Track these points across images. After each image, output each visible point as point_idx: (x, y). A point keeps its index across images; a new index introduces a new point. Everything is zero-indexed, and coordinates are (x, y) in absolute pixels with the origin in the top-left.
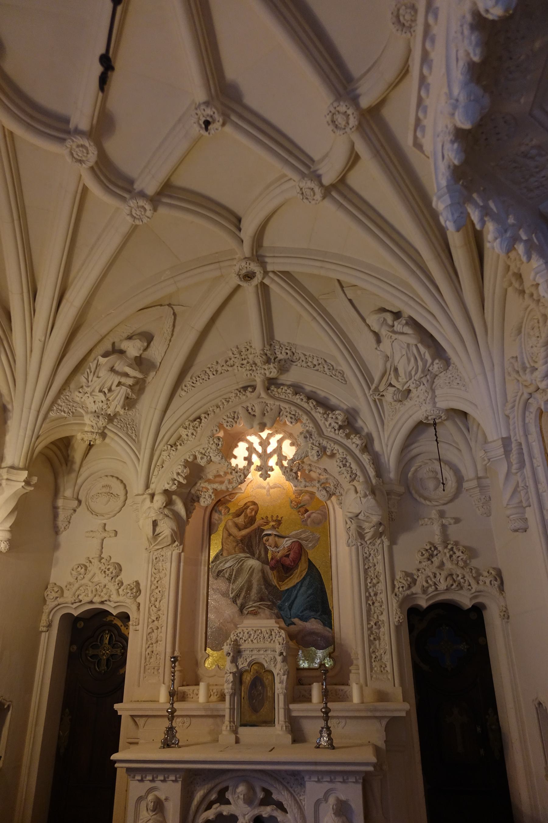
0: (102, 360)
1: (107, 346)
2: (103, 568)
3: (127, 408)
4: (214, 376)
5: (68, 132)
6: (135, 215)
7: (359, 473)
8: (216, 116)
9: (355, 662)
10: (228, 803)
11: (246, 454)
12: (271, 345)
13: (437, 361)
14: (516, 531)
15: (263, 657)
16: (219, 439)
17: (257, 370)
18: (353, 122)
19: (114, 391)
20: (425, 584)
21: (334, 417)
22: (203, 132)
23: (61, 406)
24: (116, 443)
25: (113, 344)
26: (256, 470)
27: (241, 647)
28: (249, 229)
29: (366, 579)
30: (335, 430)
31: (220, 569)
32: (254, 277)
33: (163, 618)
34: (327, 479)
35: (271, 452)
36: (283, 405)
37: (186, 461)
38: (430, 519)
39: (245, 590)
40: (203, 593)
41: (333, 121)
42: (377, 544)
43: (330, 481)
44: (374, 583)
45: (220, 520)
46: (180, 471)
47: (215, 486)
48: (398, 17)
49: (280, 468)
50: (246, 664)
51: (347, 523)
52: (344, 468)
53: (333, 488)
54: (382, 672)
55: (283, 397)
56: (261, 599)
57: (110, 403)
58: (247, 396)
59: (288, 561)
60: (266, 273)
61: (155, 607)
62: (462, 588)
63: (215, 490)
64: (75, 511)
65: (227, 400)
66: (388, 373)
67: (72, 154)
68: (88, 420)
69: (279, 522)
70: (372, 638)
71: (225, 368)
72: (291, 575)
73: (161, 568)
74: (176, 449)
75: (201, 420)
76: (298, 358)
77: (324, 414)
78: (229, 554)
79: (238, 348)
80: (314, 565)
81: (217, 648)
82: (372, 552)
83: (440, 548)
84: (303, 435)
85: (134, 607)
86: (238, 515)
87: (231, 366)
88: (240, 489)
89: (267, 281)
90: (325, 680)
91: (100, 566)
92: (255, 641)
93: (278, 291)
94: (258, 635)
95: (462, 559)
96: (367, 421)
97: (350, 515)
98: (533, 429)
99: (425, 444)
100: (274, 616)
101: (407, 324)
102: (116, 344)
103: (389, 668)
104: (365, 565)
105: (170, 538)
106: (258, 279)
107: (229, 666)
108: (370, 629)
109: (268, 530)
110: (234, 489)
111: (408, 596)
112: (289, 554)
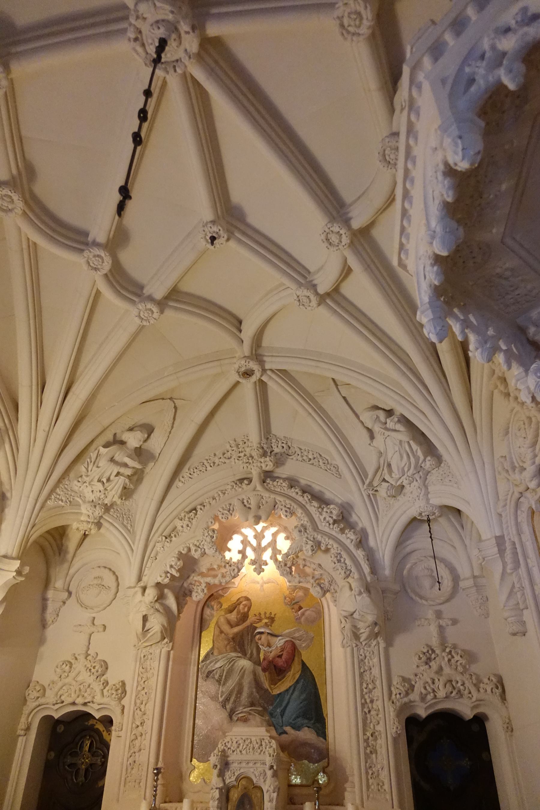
0: (103, 450)
1: (108, 436)
2: (89, 666)
3: (124, 498)
4: (211, 468)
5: (87, 244)
6: (143, 317)
7: (353, 570)
8: (221, 232)
9: (350, 779)
11: (241, 547)
12: (267, 439)
13: (429, 458)
14: (514, 634)
15: (252, 770)
16: (213, 531)
17: (253, 462)
18: (345, 240)
19: (112, 480)
20: (424, 691)
21: (328, 511)
22: (209, 246)
23: (59, 495)
24: (111, 534)
25: (115, 434)
26: (250, 564)
27: (229, 759)
28: (248, 331)
29: (361, 684)
30: (330, 524)
31: (210, 669)
32: (253, 374)
33: (148, 723)
34: (321, 575)
35: (265, 546)
36: (278, 498)
37: (180, 553)
38: (426, 619)
39: (235, 693)
40: (192, 696)
41: (328, 240)
42: (373, 645)
43: (324, 577)
44: (369, 689)
45: (212, 615)
46: (173, 564)
48: (384, 155)
49: (274, 562)
50: (233, 779)
51: (341, 622)
52: (339, 564)
53: (327, 584)
54: (379, 790)
55: (279, 490)
56: (252, 704)
57: (108, 492)
58: (243, 489)
59: (280, 662)
60: (264, 371)
61: (140, 710)
62: (461, 696)
63: (208, 584)
64: (64, 603)
65: (224, 492)
66: (381, 469)
67: (88, 263)
68: (85, 509)
70: (368, 751)
71: (223, 460)
72: (283, 678)
73: (149, 668)
74: (171, 541)
75: (197, 511)
76: (294, 452)
77: (318, 508)
78: (220, 653)
79: (235, 441)
80: (308, 668)
81: (203, 759)
82: (367, 654)
83: (438, 652)
84: (297, 529)
85: (118, 710)
87: (229, 458)
88: (234, 583)
89: (264, 378)
90: (318, 799)
91: (86, 663)
92: (244, 752)
93: (275, 387)
94: (247, 745)
95: (461, 664)
96: (361, 516)
97: (345, 614)
98: (526, 529)
99: (420, 540)
100: (265, 724)
101: (399, 421)
102: (117, 435)
103: (386, 787)
104: (360, 668)
105: (159, 635)
106: (257, 377)
107: (215, 781)
108: (366, 741)
109: (261, 627)
110: (227, 583)
111: (405, 704)
112: (282, 655)
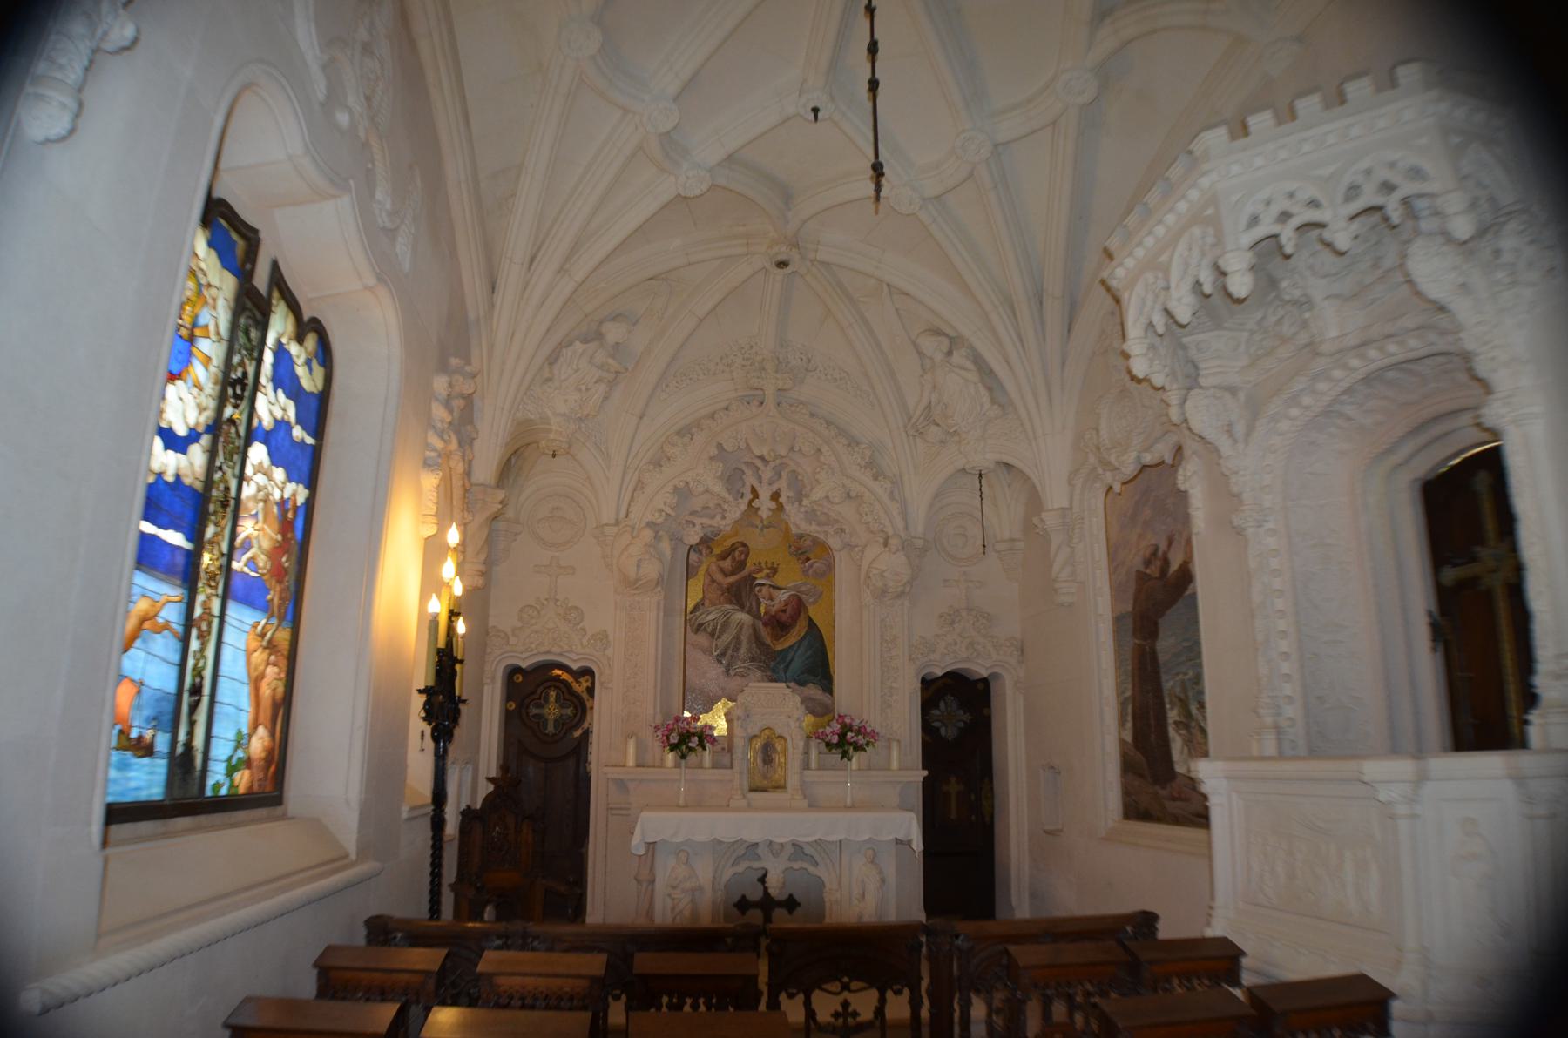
10: (759, 858)
37: (676, 489)
45: (700, 561)
47: (704, 520)
56: (753, 659)
59: (784, 618)
69: (774, 570)
83: (964, 613)
86: (723, 557)
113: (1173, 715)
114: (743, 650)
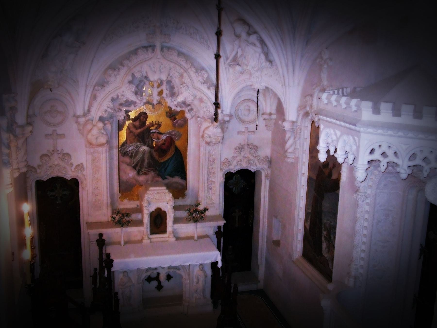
59: (164, 147)
78: (131, 143)
86: (135, 119)
109: (153, 129)
113: (324, 233)
114: (146, 163)
